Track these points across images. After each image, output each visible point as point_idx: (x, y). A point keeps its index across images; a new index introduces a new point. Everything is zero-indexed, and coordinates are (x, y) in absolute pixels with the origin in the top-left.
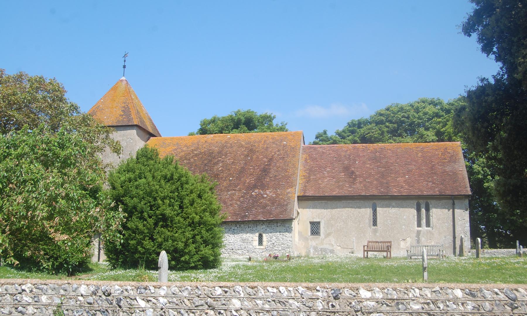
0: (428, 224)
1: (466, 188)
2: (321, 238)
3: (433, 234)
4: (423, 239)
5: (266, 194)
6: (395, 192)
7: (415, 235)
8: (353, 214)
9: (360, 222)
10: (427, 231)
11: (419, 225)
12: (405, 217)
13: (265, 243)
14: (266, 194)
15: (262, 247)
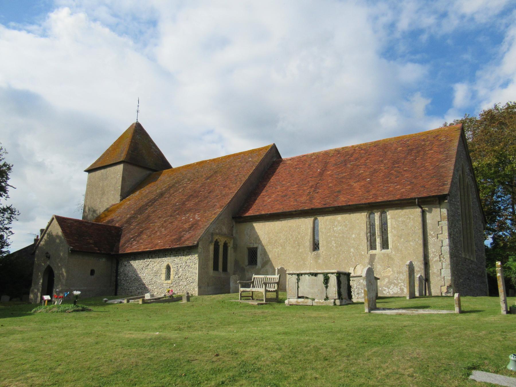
0: (385, 245)
1: (444, 185)
2: (257, 267)
3: (393, 259)
4: (379, 267)
5: (194, 218)
6: (342, 201)
7: (367, 261)
8: (291, 235)
9: (299, 246)
10: (383, 254)
11: (372, 246)
12: (354, 236)
13: (172, 277)
14: (194, 218)
15: (169, 281)
